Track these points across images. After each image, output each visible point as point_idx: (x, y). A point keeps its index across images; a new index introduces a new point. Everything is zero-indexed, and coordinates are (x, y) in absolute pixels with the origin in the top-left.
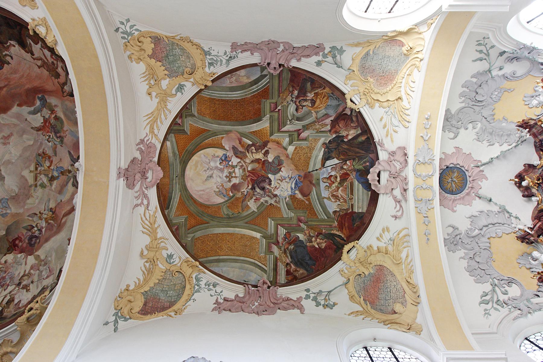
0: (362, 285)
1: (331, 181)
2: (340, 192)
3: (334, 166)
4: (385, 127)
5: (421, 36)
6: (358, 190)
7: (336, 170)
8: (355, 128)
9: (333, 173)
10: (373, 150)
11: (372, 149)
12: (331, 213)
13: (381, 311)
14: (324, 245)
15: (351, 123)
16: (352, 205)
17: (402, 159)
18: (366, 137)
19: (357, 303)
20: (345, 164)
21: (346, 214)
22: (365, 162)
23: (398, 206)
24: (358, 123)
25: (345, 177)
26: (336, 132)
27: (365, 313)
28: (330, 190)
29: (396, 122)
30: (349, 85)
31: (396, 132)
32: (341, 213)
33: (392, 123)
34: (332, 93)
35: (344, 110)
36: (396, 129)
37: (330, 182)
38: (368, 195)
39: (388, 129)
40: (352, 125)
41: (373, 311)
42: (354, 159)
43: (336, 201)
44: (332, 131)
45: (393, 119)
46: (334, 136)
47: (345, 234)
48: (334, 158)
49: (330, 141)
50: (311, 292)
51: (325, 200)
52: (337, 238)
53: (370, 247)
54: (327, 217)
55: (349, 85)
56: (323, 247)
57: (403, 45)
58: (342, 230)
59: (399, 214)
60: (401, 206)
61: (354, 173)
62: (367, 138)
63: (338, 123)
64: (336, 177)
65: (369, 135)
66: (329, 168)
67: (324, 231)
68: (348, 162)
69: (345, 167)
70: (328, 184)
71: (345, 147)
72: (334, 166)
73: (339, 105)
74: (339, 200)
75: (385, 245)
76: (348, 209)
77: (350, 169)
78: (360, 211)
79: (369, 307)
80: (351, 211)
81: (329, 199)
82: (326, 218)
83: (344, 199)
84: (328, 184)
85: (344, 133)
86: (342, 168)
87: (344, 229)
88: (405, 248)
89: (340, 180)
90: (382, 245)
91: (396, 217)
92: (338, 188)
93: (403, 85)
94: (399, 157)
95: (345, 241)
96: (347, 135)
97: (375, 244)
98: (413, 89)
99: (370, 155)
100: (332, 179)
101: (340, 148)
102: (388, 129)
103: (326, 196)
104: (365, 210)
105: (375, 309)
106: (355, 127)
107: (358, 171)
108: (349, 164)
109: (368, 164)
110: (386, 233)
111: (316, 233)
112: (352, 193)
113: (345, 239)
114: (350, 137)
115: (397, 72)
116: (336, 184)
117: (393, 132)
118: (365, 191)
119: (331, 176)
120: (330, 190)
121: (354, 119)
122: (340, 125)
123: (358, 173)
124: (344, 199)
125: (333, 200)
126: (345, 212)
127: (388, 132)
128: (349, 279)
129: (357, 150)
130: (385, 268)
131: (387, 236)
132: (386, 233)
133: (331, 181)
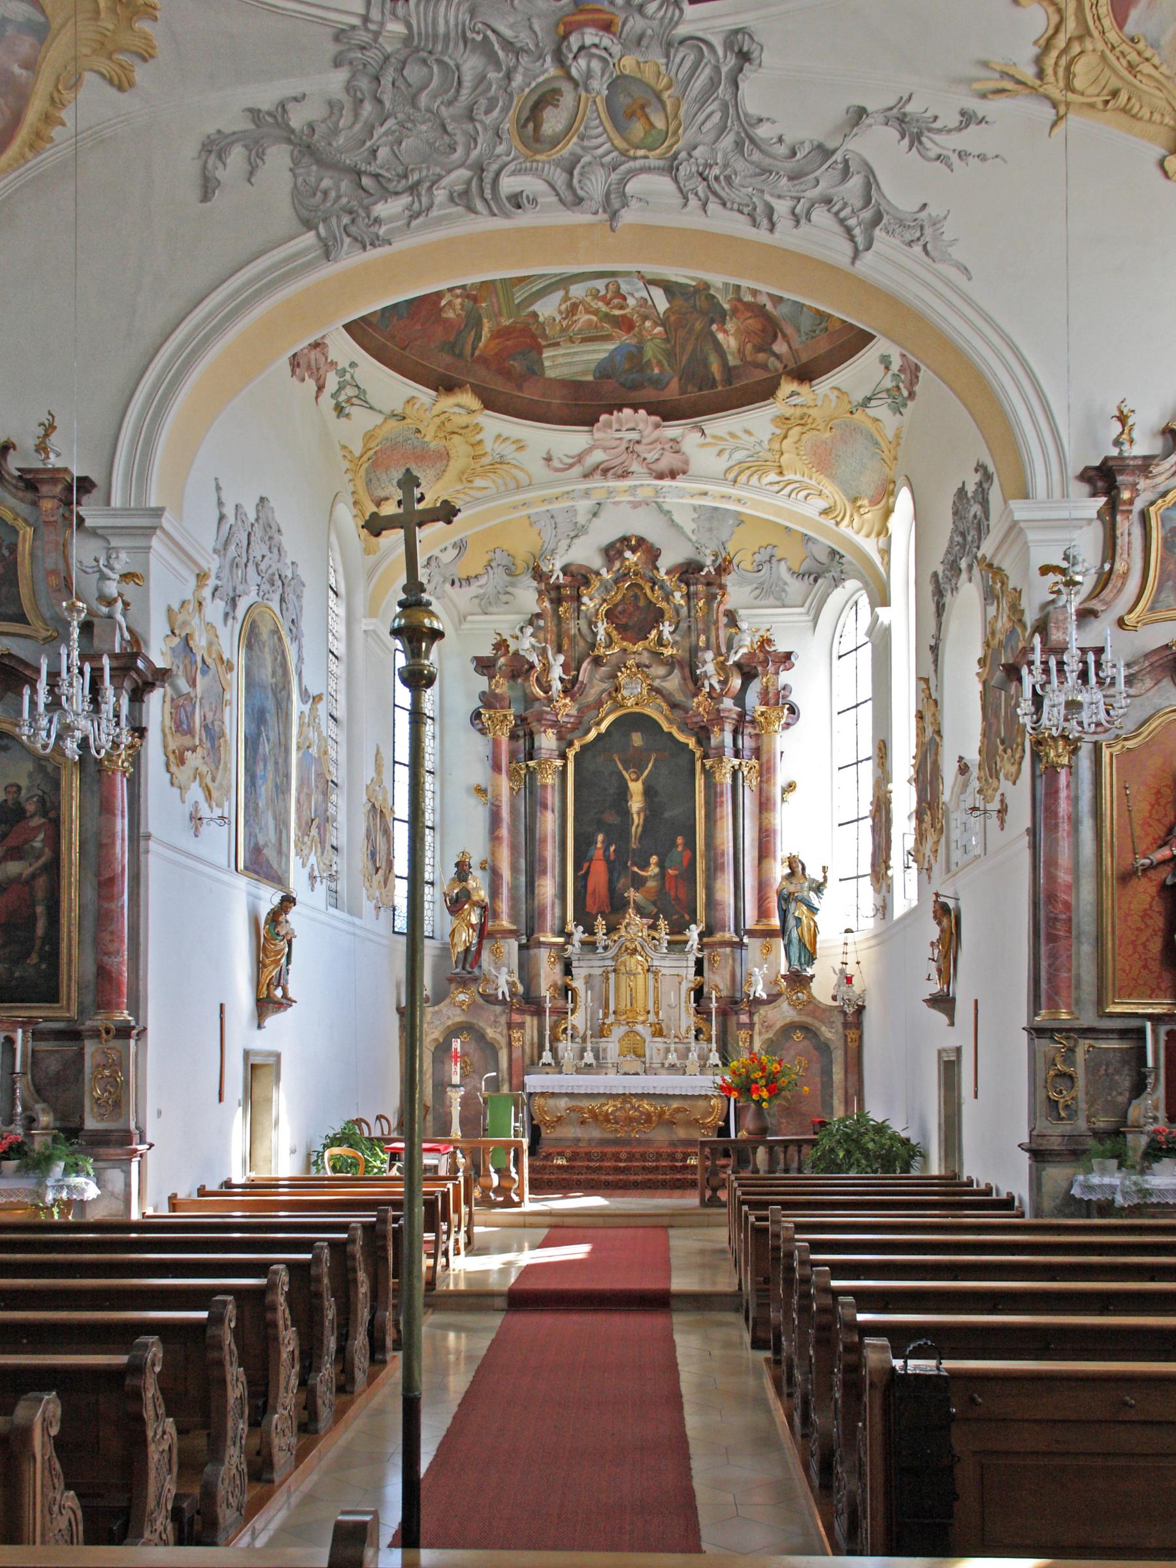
0: (400, 439)
1: (611, 299)
2: (583, 318)
3: (650, 302)
4: (732, 435)
5: (873, 535)
6: (594, 351)
7: (641, 306)
8: (741, 351)
9: (631, 302)
10: (685, 393)
11: (690, 388)
12: (531, 309)
13: (369, 482)
14: (451, 315)
15: (754, 346)
16: (557, 344)
17: (663, 465)
18: (718, 377)
19: (365, 446)
20: (656, 324)
21: (534, 337)
22: (659, 363)
23: (571, 461)
24: (749, 363)
25: (626, 324)
26: (735, 311)
27: (356, 462)
28: (589, 299)
29: (739, 456)
30: (828, 392)
31: (720, 453)
32: (533, 328)
33: (737, 449)
34: (826, 329)
35: (784, 336)
36: (726, 455)
37: (609, 296)
38: (584, 373)
39: (726, 440)
40: (749, 346)
41: (362, 472)
42: (667, 340)
43: (560, 312)
44: (739, 306)
45: (745, 453)
46: (726, 306)
47: (486, 346)
48: (669, 301)
49: (714, 297)
50: (352, 371)
51: (561, 293)
52: (473, 333)
53: (478, 428)
54: (519, 304)
55: (828, 392)
56: (444, 315)
57: (873, 503)
58: (497, 338)
59: (556, 464)
60: (571, 466)
61: (634, 341)
62: (714, 378)
63: (756, 316)
64: (622, 308)
65: (720, 388)
66: (645, 294)
67: (484, 305)
68: (659, 329)
69: (648, 324)
70: (603, 292)
71: (698, 326)
72: (650, 302)
73: (799, 331)
74: (564, 319)
75: (488, 450)
76: (545, 337)
77: (644, 333)
78: (547, 364)
79: (366, 465)
80: (544, 343)
81: (566, 298)
82: (516, 302)
83: (568, 327)
84: (603, 292)
85: (730, 326)
86: (645, 318)
87: (497, 341)
88: (494, 481)
89: (614, 316)
90: (489, 445)
91: (548, 459)
92: (596, 312)
93: (806, 479)
94: (668, 461)
95: (473, 354)
96: (726, 332)
97: (487, 436)
98: (793, 495)
99: (676, 380)
100: (616, 301)
101: (695, 315)
102: (726, 440)
103: (571, 294)
104: (551, 374)
105: (367, 472)
106: (744, 355)
107: (640, 349)
108: (656, 331)
109: (656, 371)
110: (514, 447)
111: (474, 293)
112: (584, 340)
113: (477, 353)
114: (720, 336)
115: (831, 477)
116: (604, 308)
117: (719, 448)
118: (593, 366)
119: (625, 298)
120: (589, 299)
121: (761, 357)
122: (750, 321)
123: (634, 350)
124: (568, 327)
125: (563, 307)
126: (538, 333)
127: (721, 439)
128: (404, 418)
129: (689, 348)
130: (445, 462)
131: (508, 450)
132: (514, 447)
133: (611, 299)
